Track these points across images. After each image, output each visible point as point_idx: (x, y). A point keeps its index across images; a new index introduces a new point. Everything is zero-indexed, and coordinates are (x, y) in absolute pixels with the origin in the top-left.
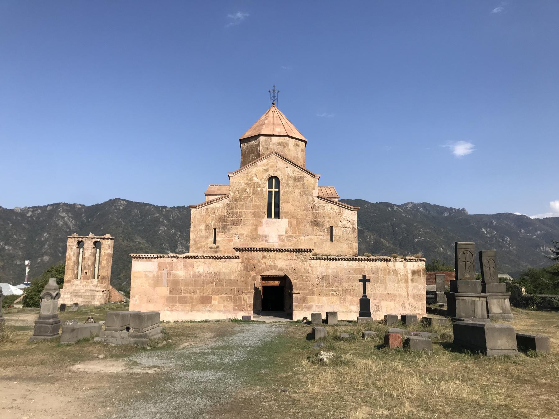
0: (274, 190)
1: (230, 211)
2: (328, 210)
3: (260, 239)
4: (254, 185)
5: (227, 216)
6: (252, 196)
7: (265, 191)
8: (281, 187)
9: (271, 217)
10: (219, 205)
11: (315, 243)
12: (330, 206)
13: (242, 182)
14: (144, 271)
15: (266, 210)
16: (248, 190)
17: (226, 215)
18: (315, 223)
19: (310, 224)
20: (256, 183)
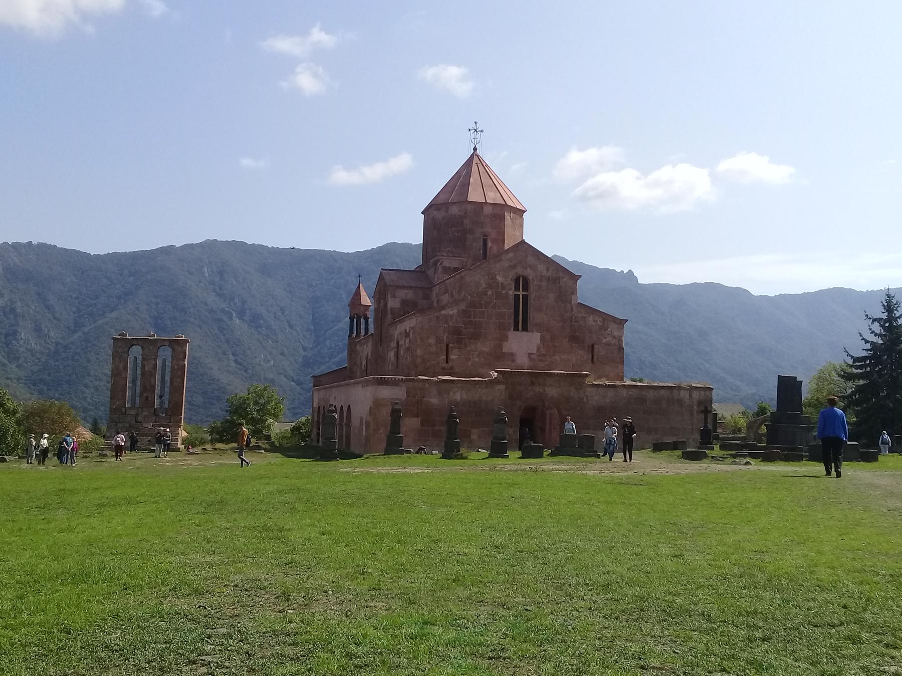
0: (521, 293)
2: (590, 323)
4: (498, 286)
8: (532, 289)
9: (519, 331)
10: (453, 312)
12: (591, 318)
13: (482, 281)
14: (390, 398)
15: (512, 321)
16: (490, 293)
18: (575, 339)
19: (567, 340)
20: (500, 283)
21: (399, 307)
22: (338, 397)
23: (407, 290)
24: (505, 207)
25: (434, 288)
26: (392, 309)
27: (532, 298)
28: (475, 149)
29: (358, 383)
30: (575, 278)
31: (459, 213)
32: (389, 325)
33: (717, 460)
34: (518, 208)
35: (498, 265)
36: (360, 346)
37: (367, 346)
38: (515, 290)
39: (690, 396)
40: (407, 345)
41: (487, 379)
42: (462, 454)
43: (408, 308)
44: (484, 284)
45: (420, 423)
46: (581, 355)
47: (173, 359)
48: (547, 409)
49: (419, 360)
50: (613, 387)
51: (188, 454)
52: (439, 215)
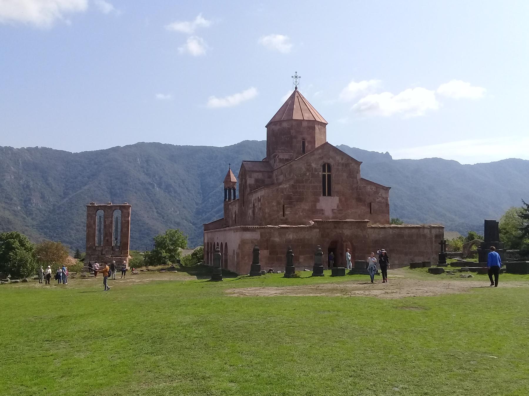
0: (326, 173)
1: (295, 191)
2: (368, 190)
3: (319, 212)
4: (313, 169)
6: (311, 179)
8: (333, 171)
9: (326, 196)
11: (359, 215)
12: (369, 187)
13: (303, 167)
14: (251, 239)
15: (322, 190)
16: (308, 174)
18: (359, 200)
20: (314, 169)
21: (254, 183)
22: (219, 237)
25: (274, 172)
26: (249, 184)
28: (296, 88)
29: (231, 230)
30: (359, 163)
31: (288, 127)
32: (248, 194)
33: (451, 274)
34: (323, 122)
35: (312, 157)
36: (231, 206)
37: (236, 206)
39: (431, 232)
40: (260, 206)
41: (308, 226)
42: (296, 275)
43: (260, 184)
45: (269, 253)
46: (364, 209)
47: (122, 217)
48: (344, 242)
49: (267, 215)
50: (383, 228)
51: (133, 274)
52: (276, 128)
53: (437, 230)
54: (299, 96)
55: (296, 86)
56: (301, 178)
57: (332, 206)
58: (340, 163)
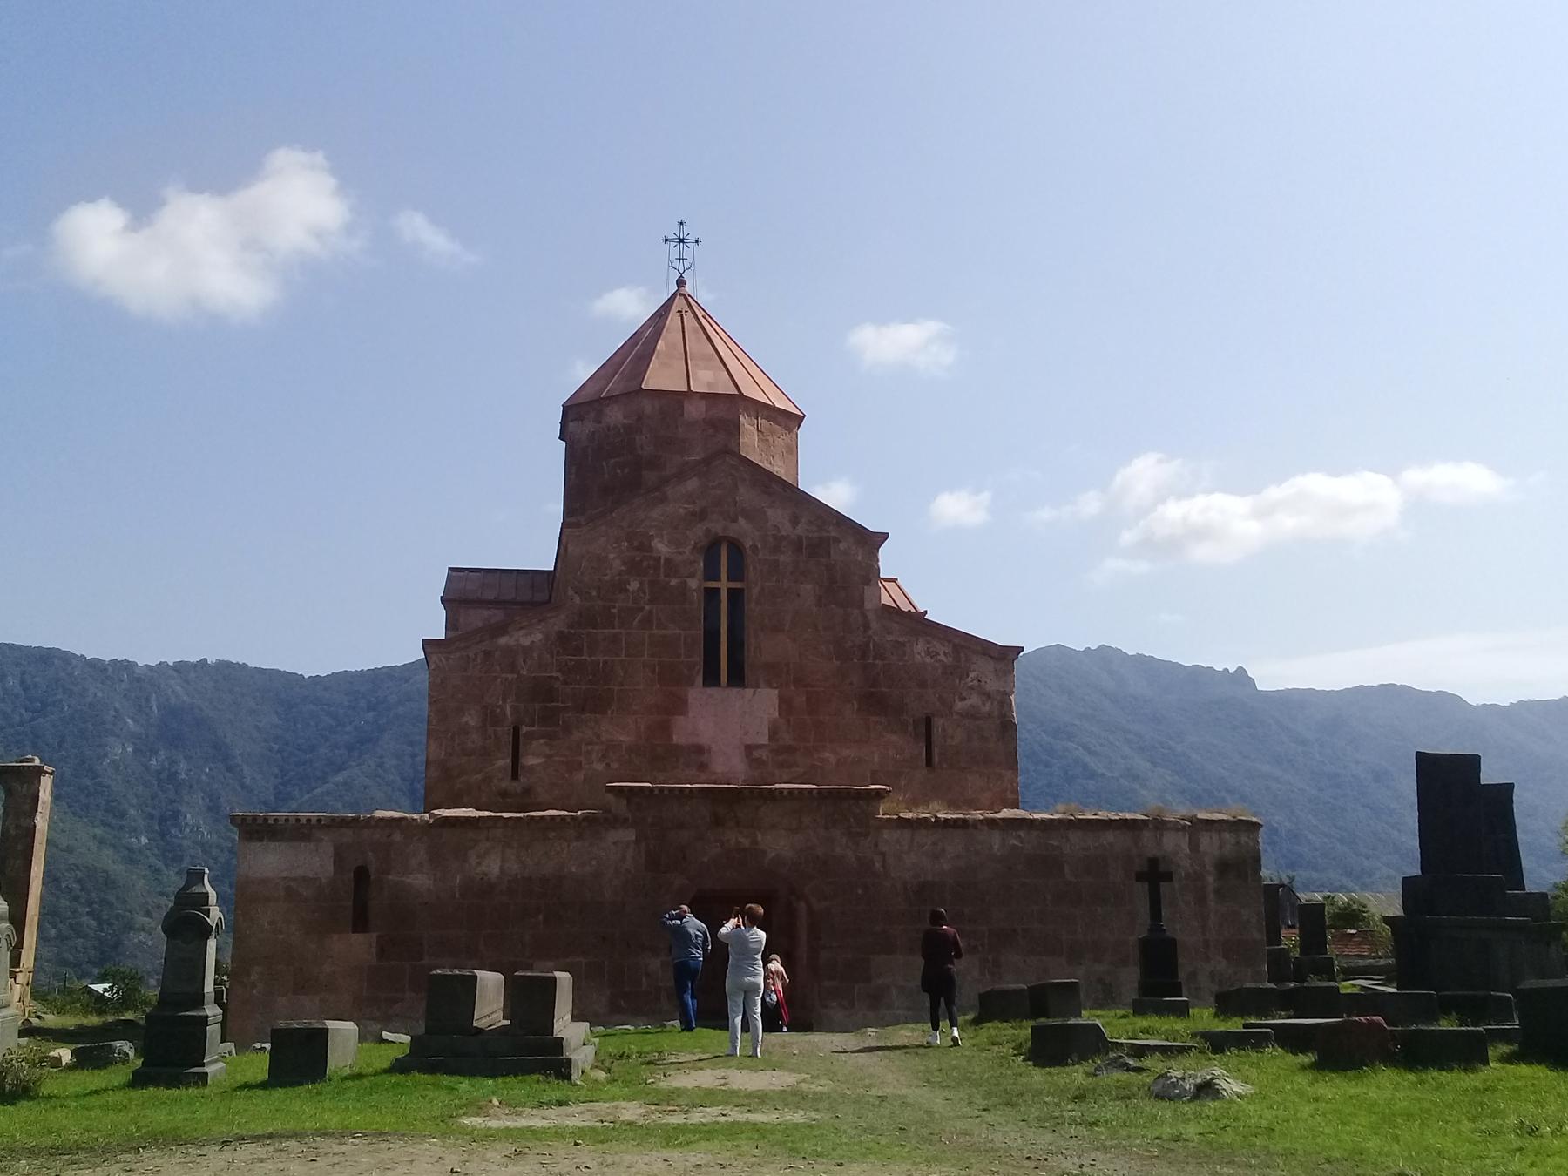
0: (724, 585)
1: (571, 660)
5: (561, 679)
6: (647, 607)
7: (694, 587)
11: (874, 773)
12: (920, 647)
13: (611, 556)
15: (698, 659)
16: (634, 585)
17: (554, 675)
18: (875, 702)
19: (856, 706)
20: (662, 561)
23: (489, 609)
24: (738, 401)
27: (754, 597)
28: (681, 283)
30: (874, 541)
35: (656, 513)
38: (708, 577)
41: (579, 813)
44: (617, 563)
52: (584, 429)
53: (1227, 835)
54: (688, 309)
55: (681, 276)
56: (600, 603)
57: (746, 733)
58: (788, 536)
